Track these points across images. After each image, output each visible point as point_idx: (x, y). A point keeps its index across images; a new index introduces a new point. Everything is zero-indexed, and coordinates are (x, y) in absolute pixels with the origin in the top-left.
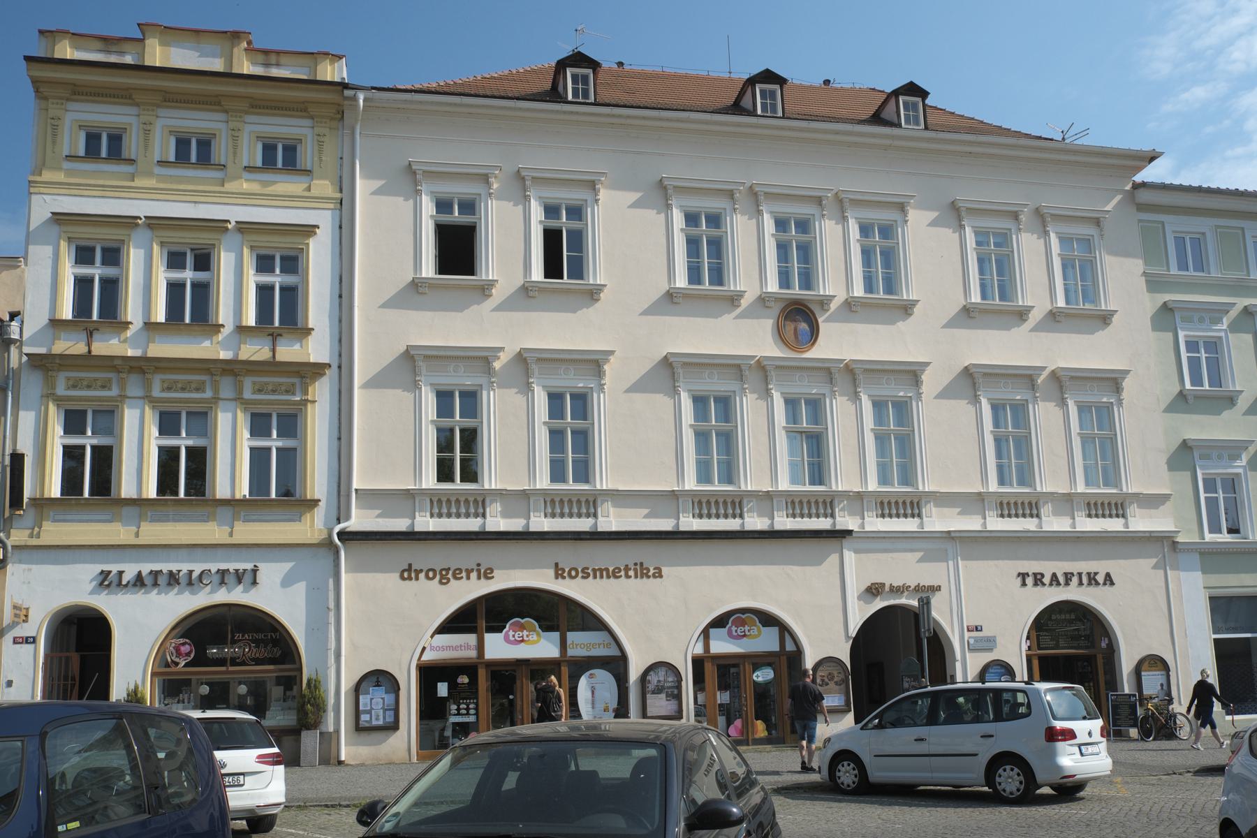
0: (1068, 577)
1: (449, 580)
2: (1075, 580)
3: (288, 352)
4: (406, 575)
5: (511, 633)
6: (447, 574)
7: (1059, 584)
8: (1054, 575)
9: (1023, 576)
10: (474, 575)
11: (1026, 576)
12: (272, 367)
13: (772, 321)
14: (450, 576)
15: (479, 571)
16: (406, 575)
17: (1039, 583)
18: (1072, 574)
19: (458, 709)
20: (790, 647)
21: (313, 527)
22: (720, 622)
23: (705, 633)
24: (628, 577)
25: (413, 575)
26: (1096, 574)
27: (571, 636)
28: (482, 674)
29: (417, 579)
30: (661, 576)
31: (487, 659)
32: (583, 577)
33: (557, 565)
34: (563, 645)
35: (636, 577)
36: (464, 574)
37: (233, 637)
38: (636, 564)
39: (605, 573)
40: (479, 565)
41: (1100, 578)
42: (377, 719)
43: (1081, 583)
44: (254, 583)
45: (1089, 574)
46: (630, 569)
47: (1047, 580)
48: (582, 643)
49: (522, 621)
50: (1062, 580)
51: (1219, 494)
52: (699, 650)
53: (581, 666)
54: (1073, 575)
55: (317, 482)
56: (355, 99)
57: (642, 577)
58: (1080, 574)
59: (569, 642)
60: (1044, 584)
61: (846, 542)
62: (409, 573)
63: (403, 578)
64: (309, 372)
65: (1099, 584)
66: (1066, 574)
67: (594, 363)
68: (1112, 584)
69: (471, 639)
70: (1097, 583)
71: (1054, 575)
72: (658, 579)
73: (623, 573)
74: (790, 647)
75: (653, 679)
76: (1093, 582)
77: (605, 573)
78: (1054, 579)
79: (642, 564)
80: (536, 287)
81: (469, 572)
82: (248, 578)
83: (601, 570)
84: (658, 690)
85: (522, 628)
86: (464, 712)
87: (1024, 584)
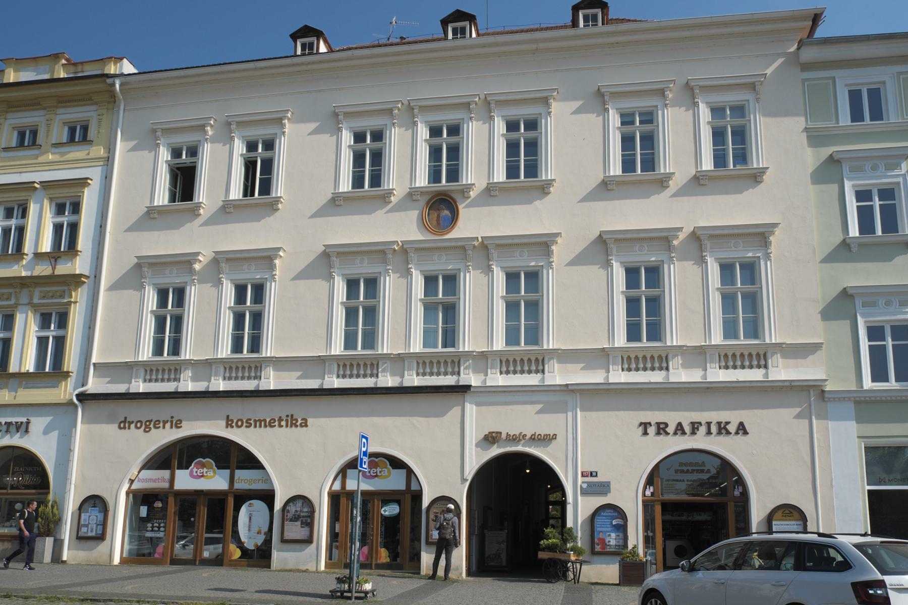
0: (695, 427)
1: (150, 429)
2: (703, 430)
3: (63, 268)
4: (122, 425)
5: (195, 470)
6: (150, 424)
7: (684, 433)
8: (680, 424)
9: (645, 426)
10: (168, 425)
11: (648, 425)
12: (53, 280)
13: (418, 211)
14: (152, 426)
15: (172, 422)
16: (122, 425)
17: (662, 431)
18: (700, 423)
19: (153, 527)
20: (414, 487)
21: (67, 391)
22: (353, 464)
23: (343, 473)
24: (280, 426)
25: (127, 425)
26: (727, 423)
27: (239, 473)
28: (171, 500)
29: (129, 428)
30: (306, 426)
31: (176, 490)
32: (247, 427)
33: (228, 417)
34: (232, 481)
35: (287, 426)
36: (161, 425)
37: (13, 469)
38: (287, 416)
39: (263, 423)
40: (172, 417)
41: (732, 428)
42: (92, 531)
43: (709, 433)
44: (27, 431)
45: (719, 423)
46: (283, 420)
47: (671, 429)
48: (245, 479)
49: (204, 461)
50: (687, 429)
51: (888, 342)
52: (337, 486)
53: (241, 498)
54: (701, 425)
56: (113, 85)
57: (291, 426)
59: (236, 477)
60: (667, 434)
61: (468, 396)
62: (124, 424)
63: (120, 428)
66: (693, 424)
67: (267, 258)
68: (746, 433)
69: (166, 474)
70: (728, 433)
71: (680, 424)
72: (304, 428)
73: (277, 423)
74: (414, 487)
75: (292, 508)
76: (723, 431)
77: (263, 423)
78: (680, 429)
79: (292, 416)
80: (230, 204)
81: (165, 422)
82: (23, 427)
83: (260, 421)
84: (295, 519)
85: (203, 466)
86: (156, 529)
87: (645, 433)
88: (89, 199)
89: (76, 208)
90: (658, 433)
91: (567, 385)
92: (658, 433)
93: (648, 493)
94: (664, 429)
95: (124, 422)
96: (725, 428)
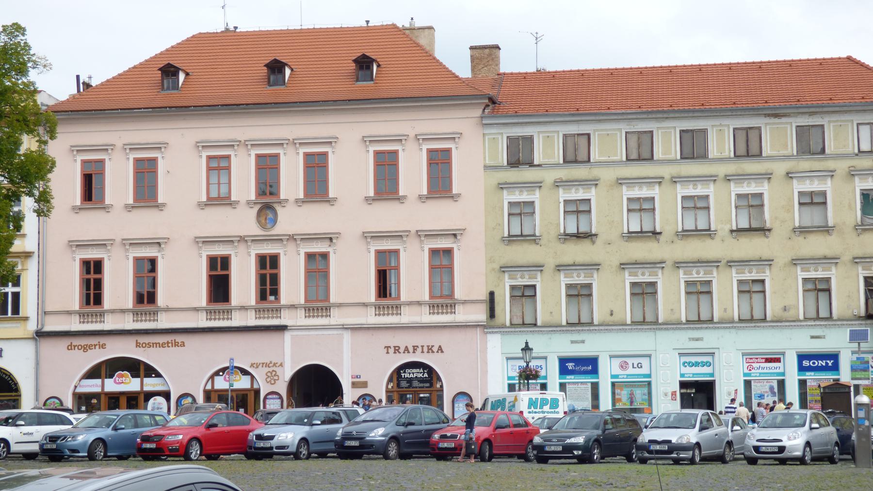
0: (415, 348)
2: (420, 350)
4: (70, 347)
7: (409, 352)
8: (406, 347)
9: (388, 347)
14: (88, 348)
15: (99, 345)
16: (70, 347)
18: (417, 346)
22: (217, 373)
25: (73, 348)
26: (433, 346)
29: (74, 349)
36: (93, 347)
41: (435, 349)
43: (423, 352)
45: (428, 346)
47: (402, 350)
50: (411, 350)
58: (422, 346)
62: (70, 347)
63: (68, 349)
66: (414, 347)
68: (442, 352)
70: (433, 352)
71: (406, 347)
76: (430, 351)
78: (407, 349)
81: (95, 345)
87: (388, 353)
90: (395, 353)
92: (395, 353)
93: (390, 387)
94: (398, 350)
95: (71, 345)
96: (431, 349)
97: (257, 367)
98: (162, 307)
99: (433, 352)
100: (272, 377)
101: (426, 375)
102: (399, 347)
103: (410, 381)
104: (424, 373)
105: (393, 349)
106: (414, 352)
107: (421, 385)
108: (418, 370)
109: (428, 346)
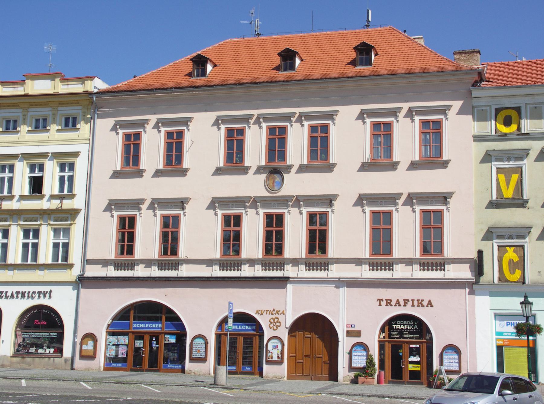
0: (406, 301)
2: (410, 303)
3: (67, 204)
7: (400, 305)
8: (398, 301)
9: (380, 300)
11: (381, 301)
18: (408, 300)
26: (423, 300)
41: (425, 303)
43: (413, 306)
44: (50, 297)
45: (418, 300)
47: (393, 303)
50: (402, 303)
54: (409, 301)
55: (75, 257)
56: (93, 98)
58: (413, 300)
64: (73, 213)
65: (424, 306)
67: (181, 203)
68: (432, 306)
70: (423, 306)
71: (398, 301)
76: (420, 305)
78: (398, 303)
82: (48, 295)
87: (380, 305)
88: (81, 164)
89: (72, 167)
90: (387, 305)
91: (339, 278)
92: (387, 305)
93: (382, 336)
94: (390, 303)
96: (421, 303)
97: (262, 314)
98: (183, 258)
99: (423, 306)
100: (275, 324)
101: (416, 327)
102: (391, 300)
103: (401, 332)
104: (414, 325)
105: (385, 301)
106: (405, 306)
107: (411, 336)
108: (408, 322)
109: (418, 300)
